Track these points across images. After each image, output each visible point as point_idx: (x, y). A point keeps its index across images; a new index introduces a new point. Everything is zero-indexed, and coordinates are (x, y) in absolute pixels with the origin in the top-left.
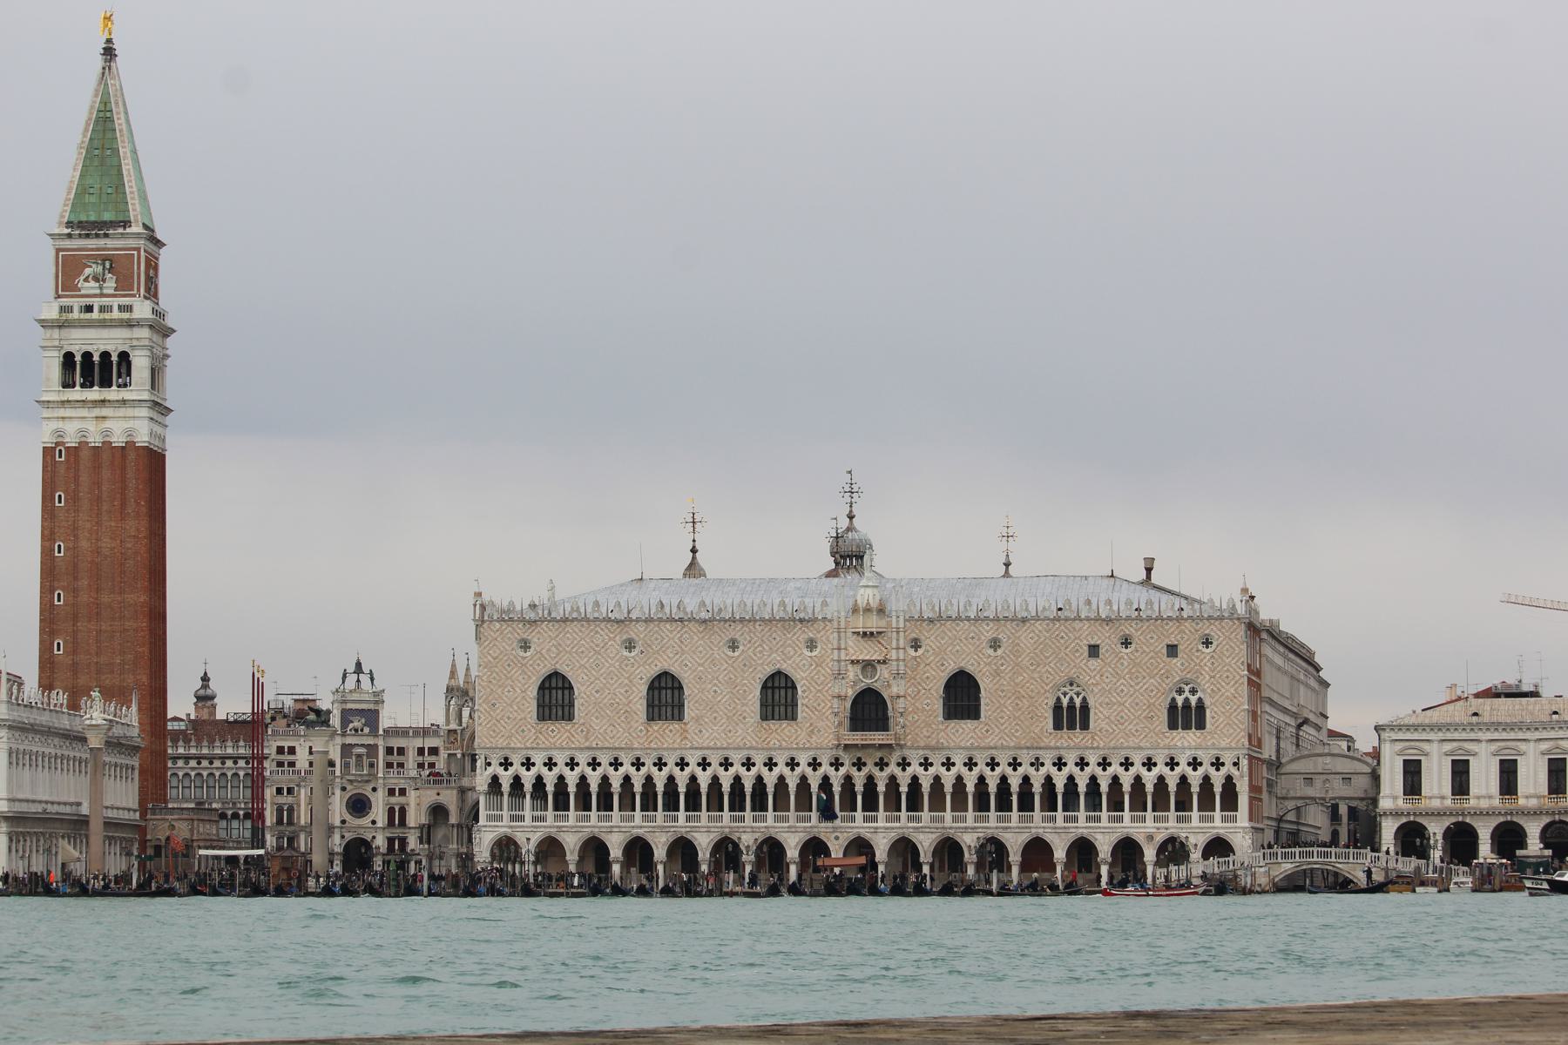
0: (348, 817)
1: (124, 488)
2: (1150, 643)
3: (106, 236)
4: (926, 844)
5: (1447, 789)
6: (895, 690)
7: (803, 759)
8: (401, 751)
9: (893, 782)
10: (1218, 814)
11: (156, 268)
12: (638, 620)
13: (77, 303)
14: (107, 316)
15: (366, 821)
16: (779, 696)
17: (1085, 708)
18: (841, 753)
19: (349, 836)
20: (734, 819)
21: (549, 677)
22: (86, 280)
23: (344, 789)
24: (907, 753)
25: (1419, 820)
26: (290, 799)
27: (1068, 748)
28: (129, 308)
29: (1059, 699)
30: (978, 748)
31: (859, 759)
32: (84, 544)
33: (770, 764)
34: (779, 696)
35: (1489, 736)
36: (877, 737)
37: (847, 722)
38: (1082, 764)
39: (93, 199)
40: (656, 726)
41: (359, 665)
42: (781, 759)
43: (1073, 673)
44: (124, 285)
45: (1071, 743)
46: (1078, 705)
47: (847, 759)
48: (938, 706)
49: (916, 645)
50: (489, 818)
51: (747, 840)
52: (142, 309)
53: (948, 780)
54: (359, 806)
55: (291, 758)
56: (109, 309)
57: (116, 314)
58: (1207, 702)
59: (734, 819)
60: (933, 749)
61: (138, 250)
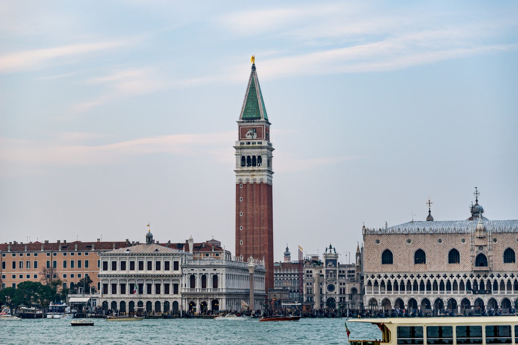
0: (328, 291)
1: (260, 196)
3: (254, 122)
4: (499, 300)
6: (489, 254)
7: (462, 275)
8: (344, 272)
11: (269, 131)
13: (245, 142)
14: (254, 145)
15: (333, 293)
16: (454, 256)
18: (473, 273)
19: (328, 297)
20: (441, 293)
22: (248, 135)
23: (327, 283)
24: (493, 273)
26: (311, 286)
28: (261, 143)
30: (515, 271)
32: (248, 212)
33: (452, 276)
34: (454, 256)
36: (484, 268)
37: (475, 264)
39: (250, 111)
41: (331, 246)
42: (455, 275)
44: (259, 136)
47: (475, 275)
48: (502, 259)
49: (495, 240)
50: (368, 293)
51: (445, 299)
52: (265, 143)
53: (506, 281)
54: (331, 288)
55: (311, 274)
56: (255, 143)
57: (257, 145)
59: (441, 293)
60: (501, 272)
61: (263, 126)
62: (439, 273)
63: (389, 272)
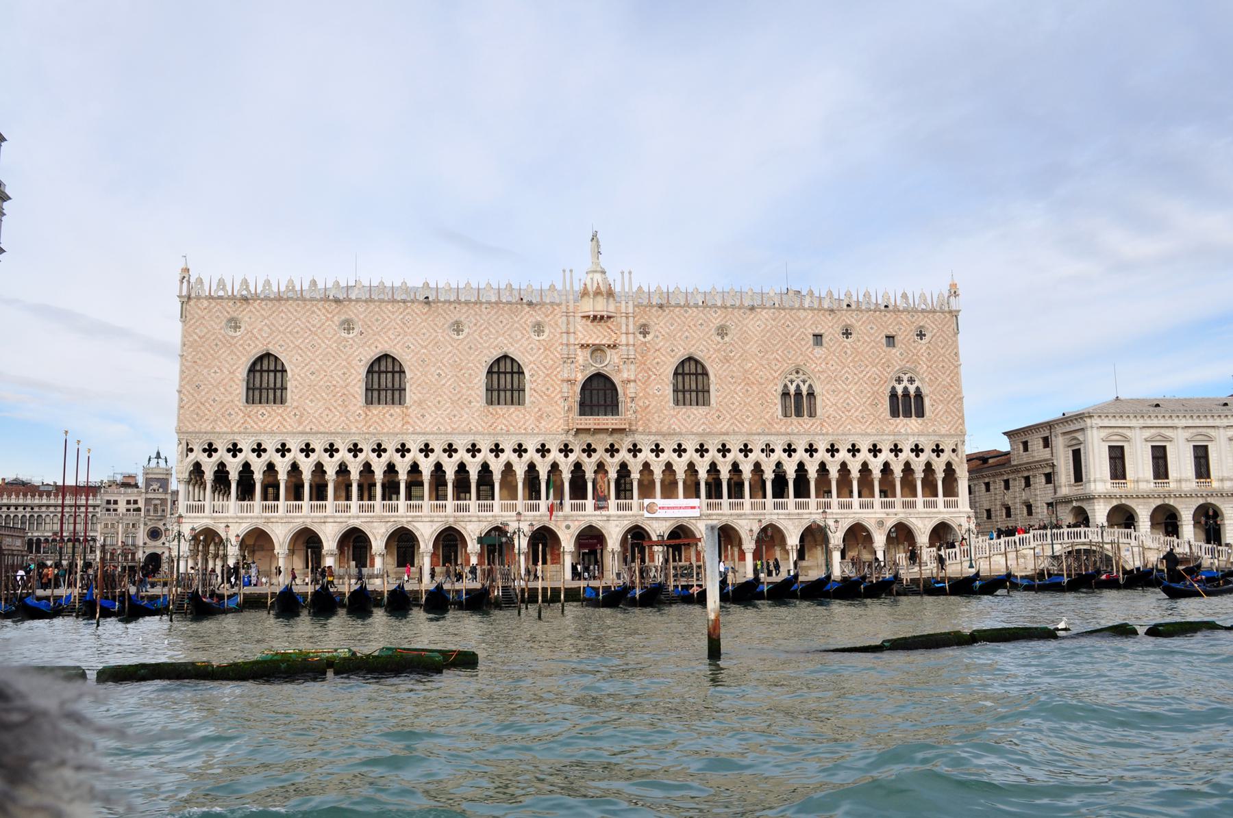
0: (147, 540)
2: (869, 333)
5: (1149, 473)
6: (625, 375)
7: (531, 446)
9: (624, 469)
10: (940, 499)
12: (357, 300)
16: (505, 380)
17: (811, 394)
19: (148, 551)
20: (459, 509)
21: (260, 359)
23: (145, 524)
25: (1171, 502)
27: (798, 434)
29: (786, 386)
30: (709, 434)
31: (589, 445)
34: (505, 380)
35: (1183, 423)
36: (608, 421)
37: (576, 407)
38: (811, 450)
40: (376, 410)
41: (158, 453)
43: (800, 360)
45: (801, 431)
46: (805, 393)
48: (669, 391)
50: (190, 509)
58: (925, 391)
59: (459, 509)
60: (664, 435)
62: (451, 439)
63: (272, 433)
